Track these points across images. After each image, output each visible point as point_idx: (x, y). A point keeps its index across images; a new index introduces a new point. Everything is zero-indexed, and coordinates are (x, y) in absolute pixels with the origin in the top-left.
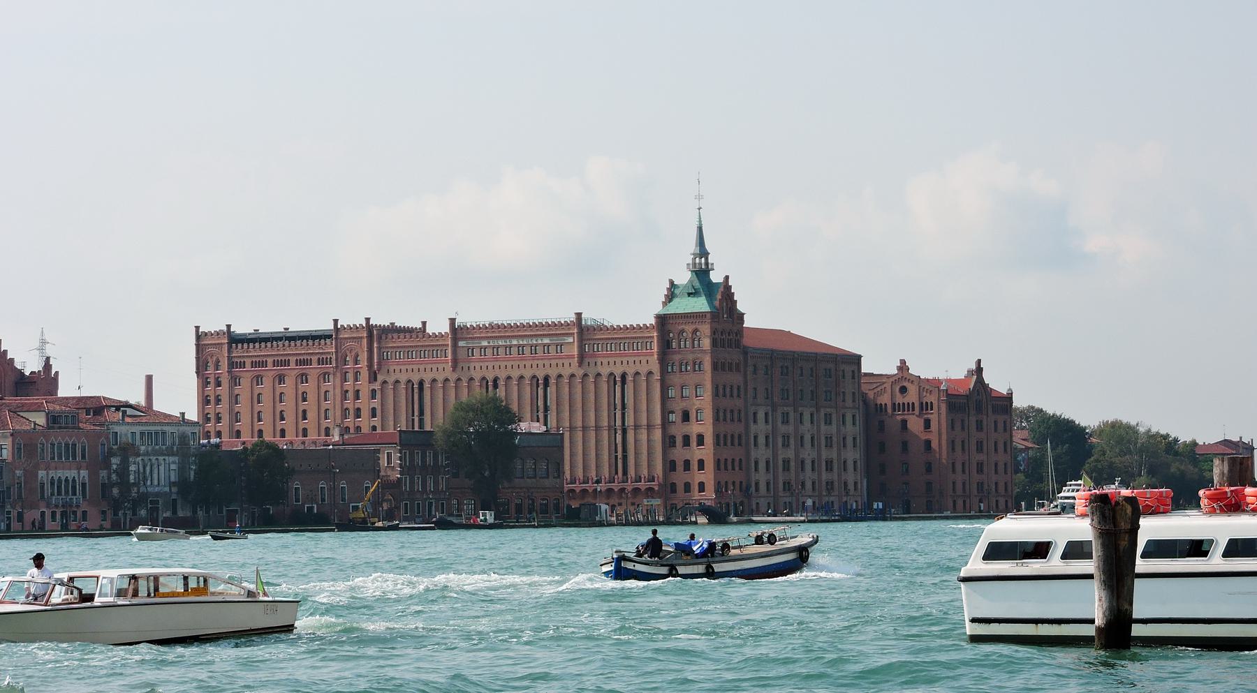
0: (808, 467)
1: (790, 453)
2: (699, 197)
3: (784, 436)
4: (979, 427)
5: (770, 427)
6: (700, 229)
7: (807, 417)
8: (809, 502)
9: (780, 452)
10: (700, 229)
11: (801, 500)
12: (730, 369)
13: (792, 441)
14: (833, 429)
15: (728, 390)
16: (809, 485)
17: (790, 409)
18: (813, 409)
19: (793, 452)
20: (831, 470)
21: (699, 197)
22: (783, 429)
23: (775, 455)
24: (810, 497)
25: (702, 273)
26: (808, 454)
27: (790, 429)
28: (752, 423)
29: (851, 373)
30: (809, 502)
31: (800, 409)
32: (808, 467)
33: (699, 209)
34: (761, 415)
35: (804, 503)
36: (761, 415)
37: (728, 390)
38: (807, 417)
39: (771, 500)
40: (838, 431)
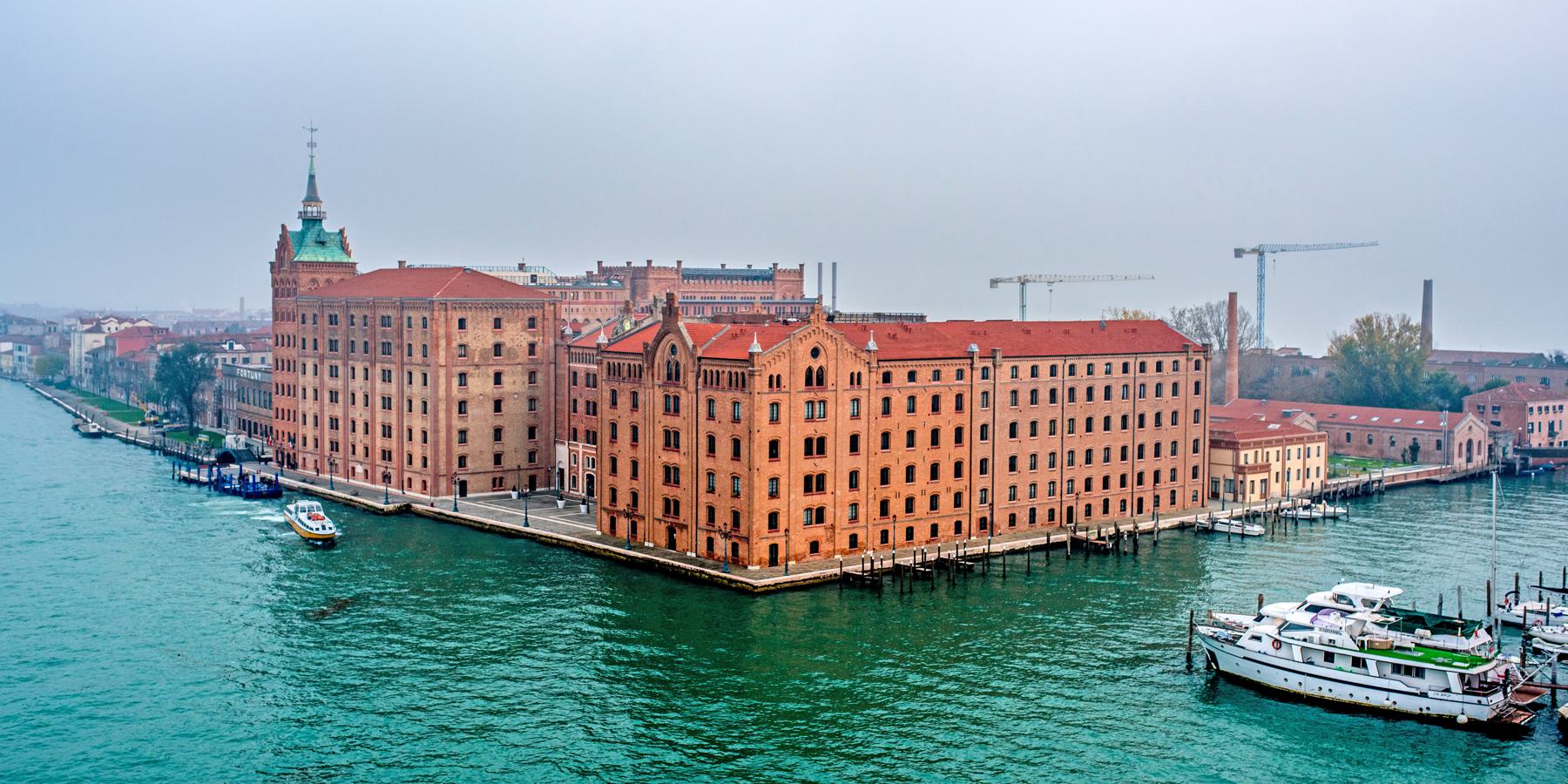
0: (360, 428)
1: (338, 411)
2: (312, 145)
3: (331, 392)
4: (672, 407)
5: (317, 380)
6: (312, 177)
7: (360, 373)
8: (359, 469)
9: (326, 408)
10: (312, 177)
11: (351, 465)
12: (289, 320)
13: (340, 397)
14: (392, 389)
15: (286, 340)
16: (360, 450)
17: (339, 363)
18: (367, 364)
19: (341, 409)
20: (390, 436)
21: (312, 145)
22: (331, 384)
23: (322, 410)
24: (361, 463)
25: (311, 221)
26: (359, 414)
27: (338, 384)
28: (300, 375)
29: (421, 322)
30: (359, 469)
31: (350, 362)
32: (360, 428)
33: (312, 157)
34: (310, 367)
35: (353, 469)
36: (310, 367)
37: (286, 340)
38: (360, 373)
39: (317, 457)
40: (401, 392)
